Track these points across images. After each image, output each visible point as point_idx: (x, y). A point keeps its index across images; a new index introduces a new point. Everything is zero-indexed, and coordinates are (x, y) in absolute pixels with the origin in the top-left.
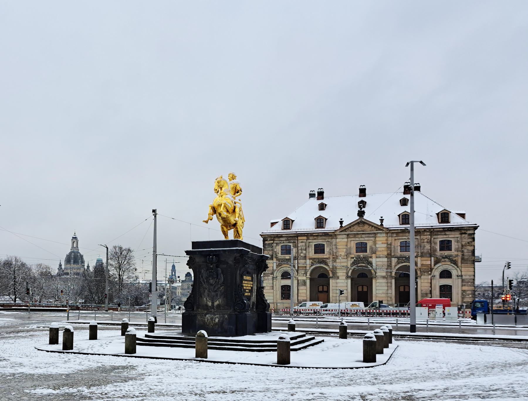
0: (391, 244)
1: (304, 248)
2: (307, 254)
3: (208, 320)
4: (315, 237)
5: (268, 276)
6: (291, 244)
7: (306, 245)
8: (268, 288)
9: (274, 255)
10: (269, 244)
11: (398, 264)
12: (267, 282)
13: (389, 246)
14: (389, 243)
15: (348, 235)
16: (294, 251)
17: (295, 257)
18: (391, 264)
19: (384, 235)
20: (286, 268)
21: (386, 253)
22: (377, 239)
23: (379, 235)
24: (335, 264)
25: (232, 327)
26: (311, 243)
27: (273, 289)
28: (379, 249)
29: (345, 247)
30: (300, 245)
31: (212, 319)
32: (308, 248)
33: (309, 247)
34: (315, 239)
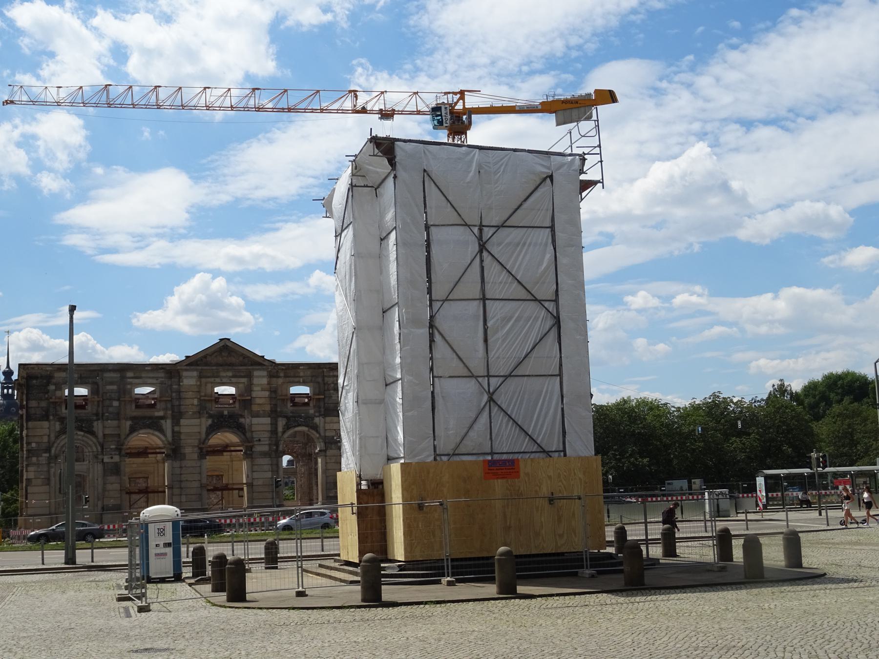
11: (288, 428)
13: (273, 395)
18: (276, 428)
21: (268, 408)
24: (176, 429)
27: (49, 484)
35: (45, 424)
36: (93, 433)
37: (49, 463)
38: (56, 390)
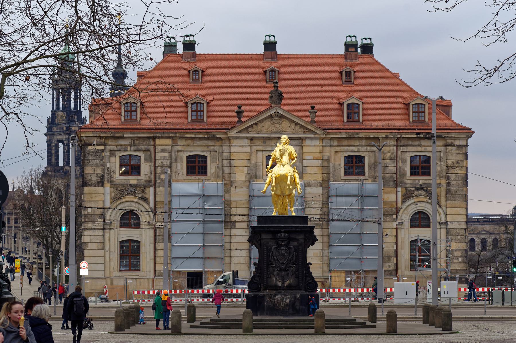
0: (328, 161)
1: (167, 163)
2: (174, 174)
3: (278, 301)
4: (189, 142)
5: (93, 222)
6: (141, 154)
7: (171, 158)
8: (95, 246)
9: (106, 176)
10: (96, 151)
12: (91, 232)
13: (326, 164)
14: (326, 158)
15: (252, 139)
16: (145, 168)
17: (150, 181)
19: (317, 142)
20: (130, 203)
21: (319, 177)
22: (305, 149)
23: (308, 142)
25: (304, 307)
26: (180, 154)
27: (104, 248)
28: (308, 170)
29: (245, 163)
30: (159, 155)
31: (282, 300)
32: (174, 164)
33: (176, 160)
34: (188, 145)
35: (100, 189)
36: (145, 200)
37: (104, 229)
38: (110, 156)
